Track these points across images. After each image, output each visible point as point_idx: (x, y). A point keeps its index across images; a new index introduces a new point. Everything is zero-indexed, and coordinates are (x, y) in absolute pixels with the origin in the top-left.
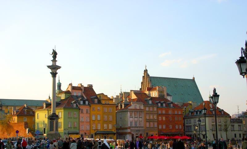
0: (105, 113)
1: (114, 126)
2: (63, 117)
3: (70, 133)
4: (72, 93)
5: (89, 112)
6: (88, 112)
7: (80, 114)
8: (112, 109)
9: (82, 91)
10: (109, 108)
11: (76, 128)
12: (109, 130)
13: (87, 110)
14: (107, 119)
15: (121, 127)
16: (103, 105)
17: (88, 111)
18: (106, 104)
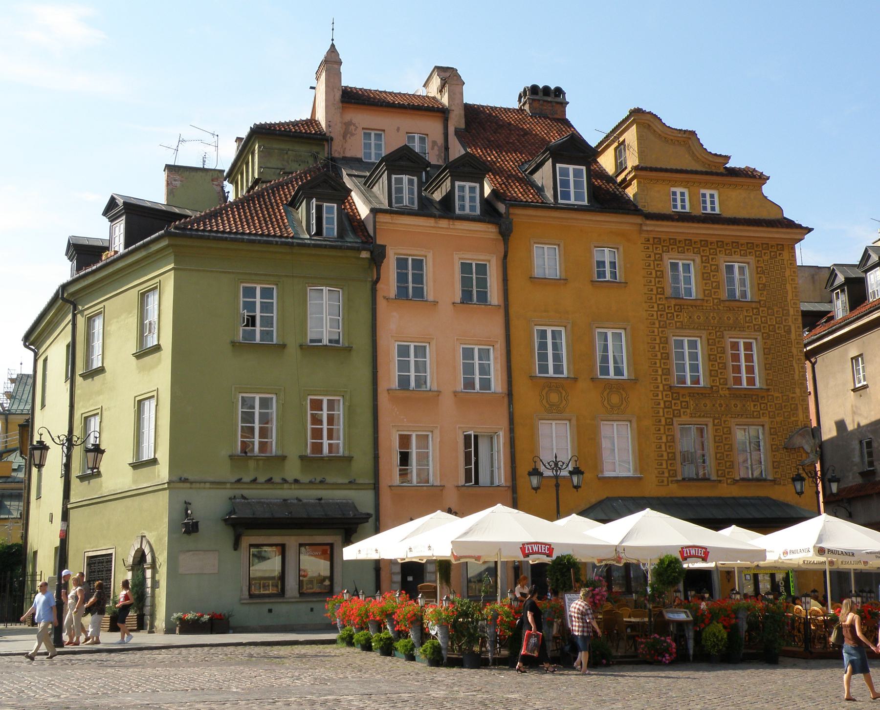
0: (680, 304)
1: (789, 448)
2: (167, 342)
3: (247, 514)
4: (336, 133)
5: (494, 296)
6: (483, 297)
7: (381, 304)
8: (760, 271)
9: (446, 121)
10: (722, 261)
11: (349, 459)
12: (735, 491)
13: (466, 268)
14: (712, 374)
15: (863, 474)
16: (651, 226)
17: (482, 283)
18: (684, 218)
